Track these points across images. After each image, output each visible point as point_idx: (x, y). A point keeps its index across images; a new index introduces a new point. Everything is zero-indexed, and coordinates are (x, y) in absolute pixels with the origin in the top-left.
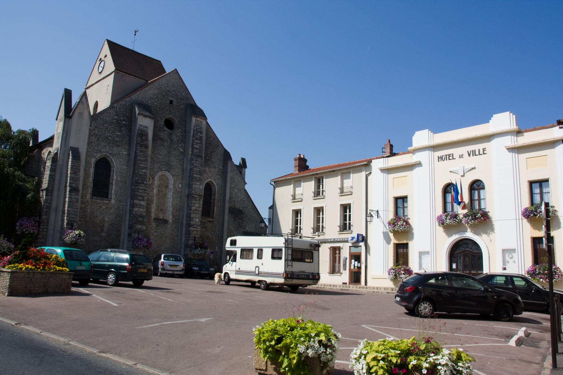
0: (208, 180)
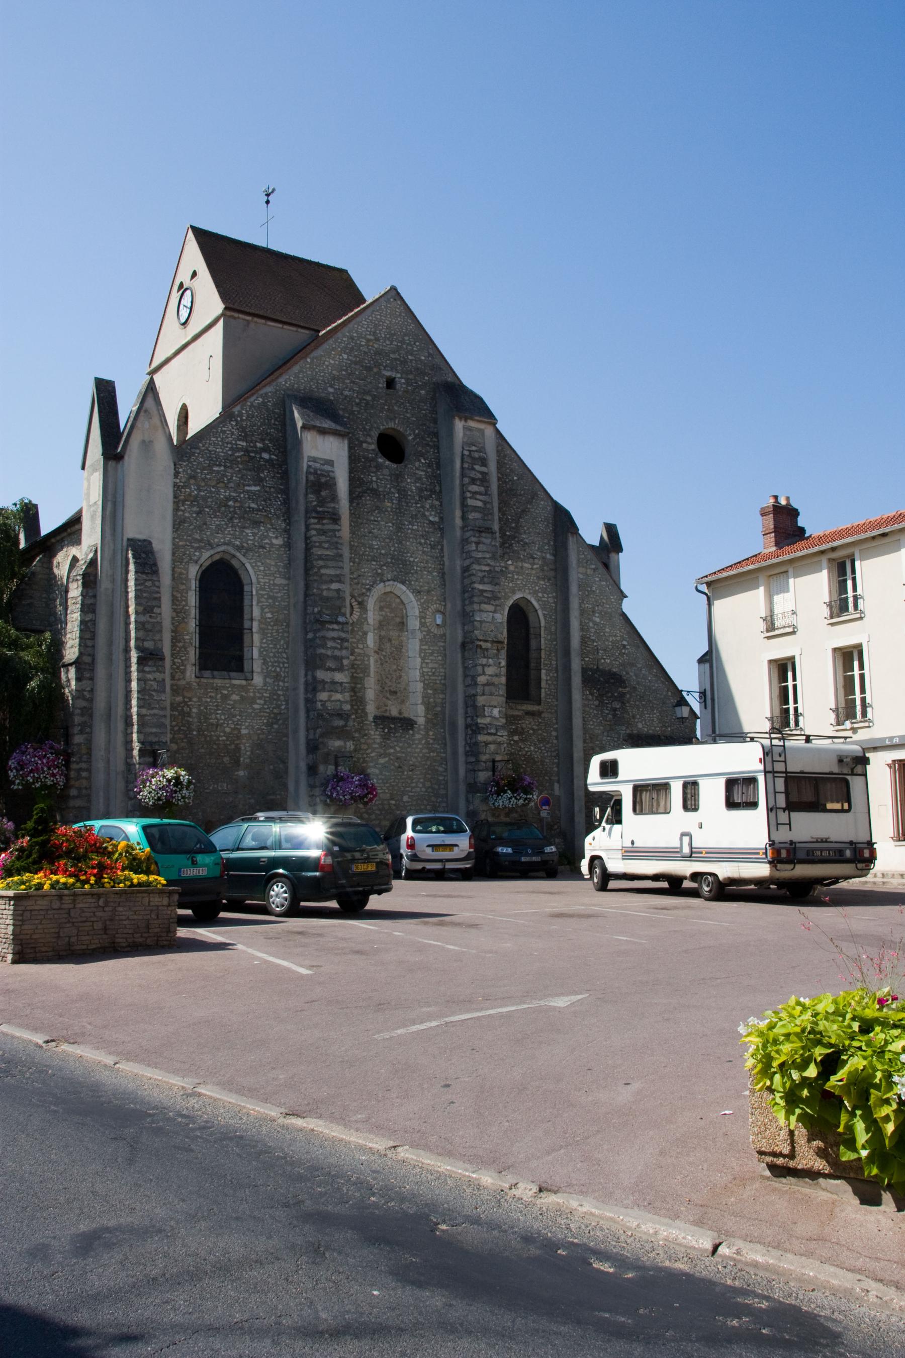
0: (518, 596)
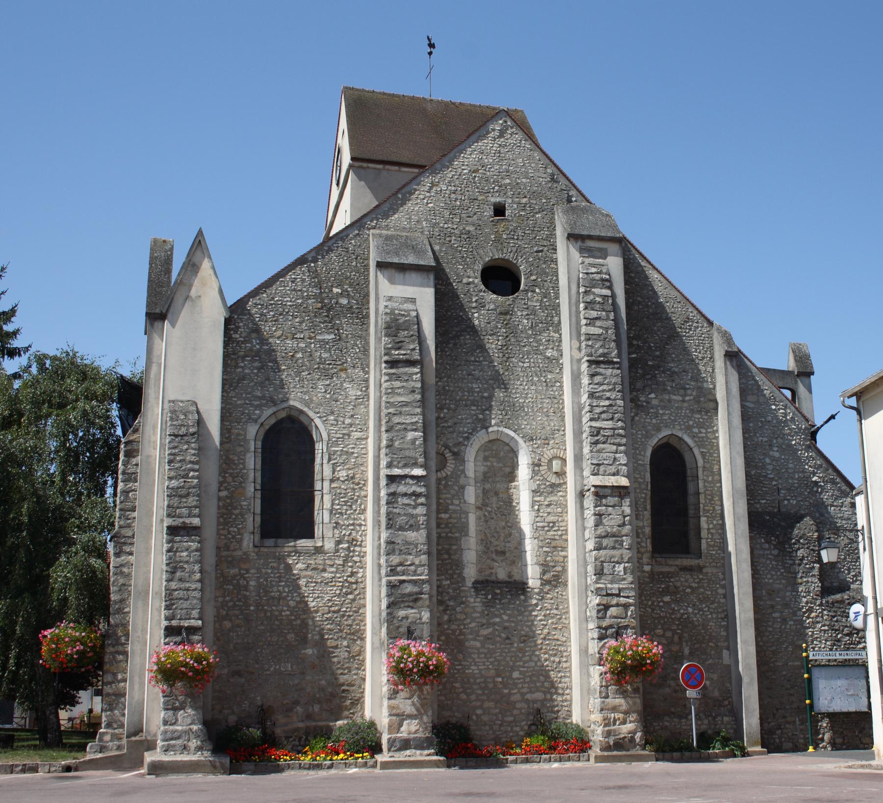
0: (665, 433)
